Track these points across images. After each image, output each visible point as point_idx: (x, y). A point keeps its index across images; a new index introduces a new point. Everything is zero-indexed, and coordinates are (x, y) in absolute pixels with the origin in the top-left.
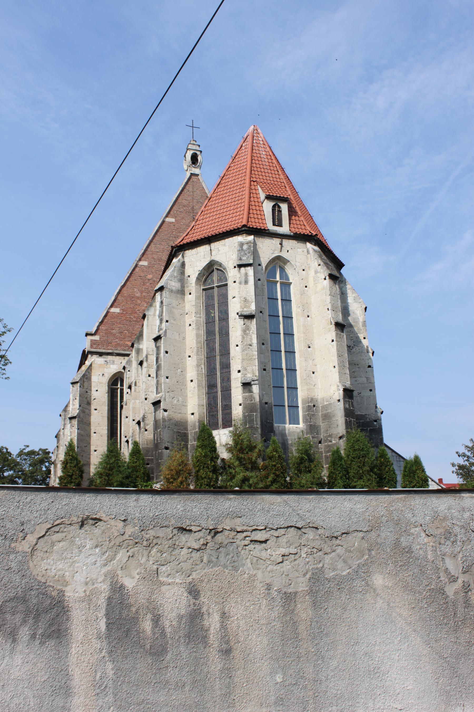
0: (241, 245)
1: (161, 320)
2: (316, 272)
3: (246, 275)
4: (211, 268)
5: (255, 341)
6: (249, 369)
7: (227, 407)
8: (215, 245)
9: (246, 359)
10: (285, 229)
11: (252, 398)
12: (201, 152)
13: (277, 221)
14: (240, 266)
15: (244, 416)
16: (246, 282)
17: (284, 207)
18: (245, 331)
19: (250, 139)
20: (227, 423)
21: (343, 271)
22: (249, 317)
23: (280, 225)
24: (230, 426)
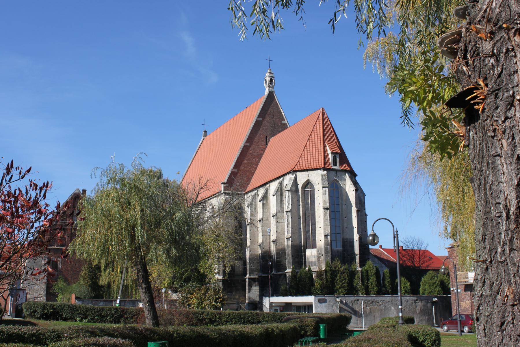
0: (322, 176)
1: (289, 204)
2: (350, 187)
3: (325, 191)
4: (308, 183)
5: (329, 218)
6: (327, 229)
7: (314, 240)
8: (310, 172)
9: (325, 225)
10: (337, 167)
11: (328, 241)
12: (274, 77)
13: (335, 164)
14: (323, 187)
15: (325, 248)
16: (325, 194)
17: (338, 156)
18: (325, 214)
19: (321, 114)
20: (314, 246)
21: (356, 178)
22: (327, 209)
23: (336, 165)
24: (315, 247)
